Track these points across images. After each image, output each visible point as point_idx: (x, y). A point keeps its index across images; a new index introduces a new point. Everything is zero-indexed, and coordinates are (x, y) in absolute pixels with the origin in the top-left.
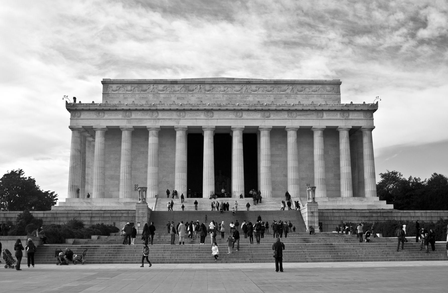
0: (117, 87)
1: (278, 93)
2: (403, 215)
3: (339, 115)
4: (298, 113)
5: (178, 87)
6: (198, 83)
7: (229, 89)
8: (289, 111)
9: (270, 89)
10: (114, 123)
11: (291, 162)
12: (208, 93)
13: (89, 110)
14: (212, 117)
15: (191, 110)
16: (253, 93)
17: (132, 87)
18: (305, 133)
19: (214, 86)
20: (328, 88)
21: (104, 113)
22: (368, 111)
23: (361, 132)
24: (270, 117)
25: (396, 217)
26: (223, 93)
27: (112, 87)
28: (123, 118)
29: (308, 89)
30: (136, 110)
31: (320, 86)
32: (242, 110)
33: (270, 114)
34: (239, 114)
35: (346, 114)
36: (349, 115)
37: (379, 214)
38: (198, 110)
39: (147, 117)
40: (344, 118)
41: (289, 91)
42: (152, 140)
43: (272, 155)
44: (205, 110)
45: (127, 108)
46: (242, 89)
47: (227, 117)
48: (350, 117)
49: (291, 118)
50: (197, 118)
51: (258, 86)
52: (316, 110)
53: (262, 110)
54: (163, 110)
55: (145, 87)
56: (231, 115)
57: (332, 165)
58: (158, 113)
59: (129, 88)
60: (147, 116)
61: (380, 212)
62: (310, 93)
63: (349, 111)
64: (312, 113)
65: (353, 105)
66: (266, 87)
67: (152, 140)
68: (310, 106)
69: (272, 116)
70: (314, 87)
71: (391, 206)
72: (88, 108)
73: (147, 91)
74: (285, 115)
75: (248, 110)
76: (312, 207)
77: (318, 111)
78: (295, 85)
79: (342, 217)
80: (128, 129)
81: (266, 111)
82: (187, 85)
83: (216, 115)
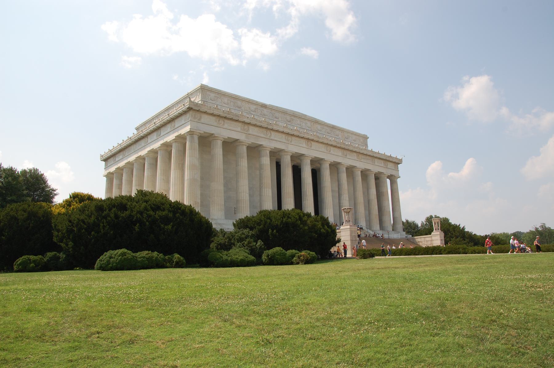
3: (382, 163)
10: (235, 135)
12: (289, 123)
13: (212, 115)
14: (311, 147)
15: (298, 136)
24: (346, 156)
30: (255, 125)
32: (332, 145)
34: (329, 148)
44: (308, 139)
45: (247, 121)
50: (301, 145)
54: (277, 131)
55: (239, 103)
63: (389, 161)
69: (348, 157)
72: (211, 112)
73: (243, 108)
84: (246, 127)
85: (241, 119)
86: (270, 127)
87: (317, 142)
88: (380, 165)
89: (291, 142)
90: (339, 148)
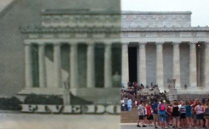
3: (190, 35)
8: (158, 32)
9: (145, 18)
11: (160, 65)
18: (168, 46)
20: (183, 16)
23: (204, 45)
24: (145, 36)
29: (170, 17)
31: (178, 16)
35: (195, 34)
41: (157, 19)
43: (146, 61)
48: (197, 36)
51: (138, 16)
52: (175, 31)
57: (185, 66)
63: (197, 31)
69: (147, 36)
70: (174, 16)
74: (155, 35)
75: (132, 32)
77: (177, 32)
81: (143, 32)
88: (188, 36)
90: (136, 32)
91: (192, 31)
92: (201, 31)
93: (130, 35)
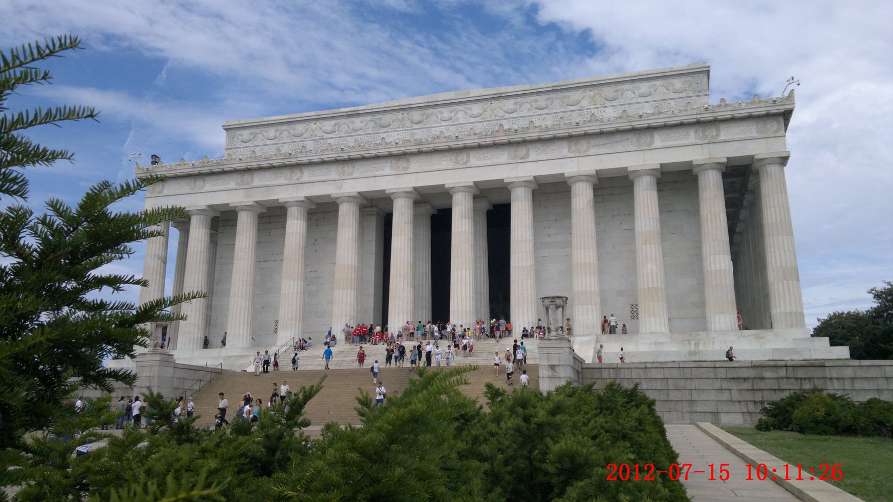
0: (251, 134)
1: (563, 110)
2: (860, 373)
3: (692, 136)
4: (593, 142)
5: (362, 122)
6: (399, 110)
7: (461, 115)
8: (570, 138)
14: (408, 168)
15: (364, 159)
16: (508, 116)
17: (277, 131)
18: (613, 188)
19: (429, 111)
20: (678, 83)
21: (204, 181)
22: (768, 116)
24: (527, 156)
25: (837, 379)
26: (447, 123)
27: (241, 135)
28: (238, 187)
30: (260, 169)
31: (659, 83)
32: (466, 149)
33: (528, 151)
34: (463, 157)
35: (711, 132)
36: (718, 135)
37: (782, 373)
38: (377, 157)
39: (282, 181)
40: (706, 141)
42: (296, 226)
46: (485, 110)
47: (436, 167)
48: (722, 137)
49: (577, 155)
50: (377, 173)
51: (519, 100)
52: (633, 130)
53: (510, 144)
54: (311, 164)
55: (300, 128)
56: (445, 162)
58: (302, 172)
59: (272, 132)
60: (281, 178)
61: (786, 366)
62: (634, 101)
64: (625, 136)
65: (727, 105)
66: (536, 101)
67: (296, 226)
68: (619, 121)
70: (644, 87)
71: (843, 352)
73: (304, 136)
74: (563, 149)
75: (480, 147)
76: (552, 351)
78: (600, 88)
79: (670, 381)
80: (247, 208)
82: (378, 116)
83: (415, 164)
84: (247, 177)
85: (227, 168)
86: (291, 161)
87: (420, 153)
89: (350, 174)
90: (495, 146)
91: (698, 123)
92: (733, 119)
93: (475, 159)
